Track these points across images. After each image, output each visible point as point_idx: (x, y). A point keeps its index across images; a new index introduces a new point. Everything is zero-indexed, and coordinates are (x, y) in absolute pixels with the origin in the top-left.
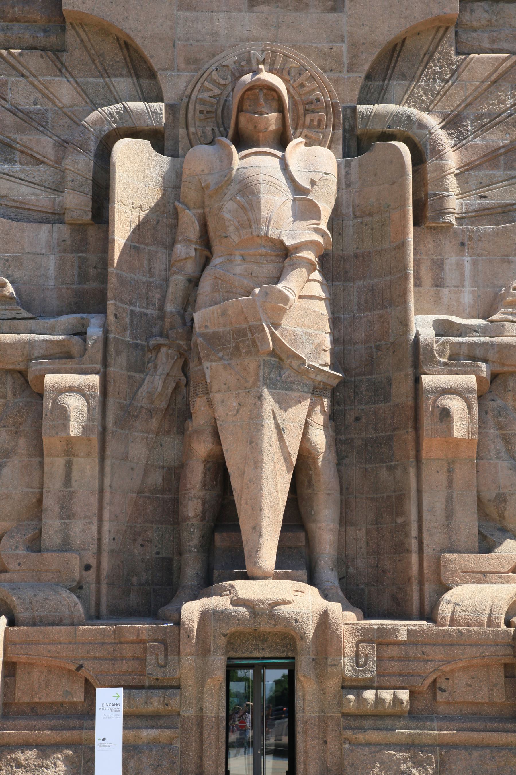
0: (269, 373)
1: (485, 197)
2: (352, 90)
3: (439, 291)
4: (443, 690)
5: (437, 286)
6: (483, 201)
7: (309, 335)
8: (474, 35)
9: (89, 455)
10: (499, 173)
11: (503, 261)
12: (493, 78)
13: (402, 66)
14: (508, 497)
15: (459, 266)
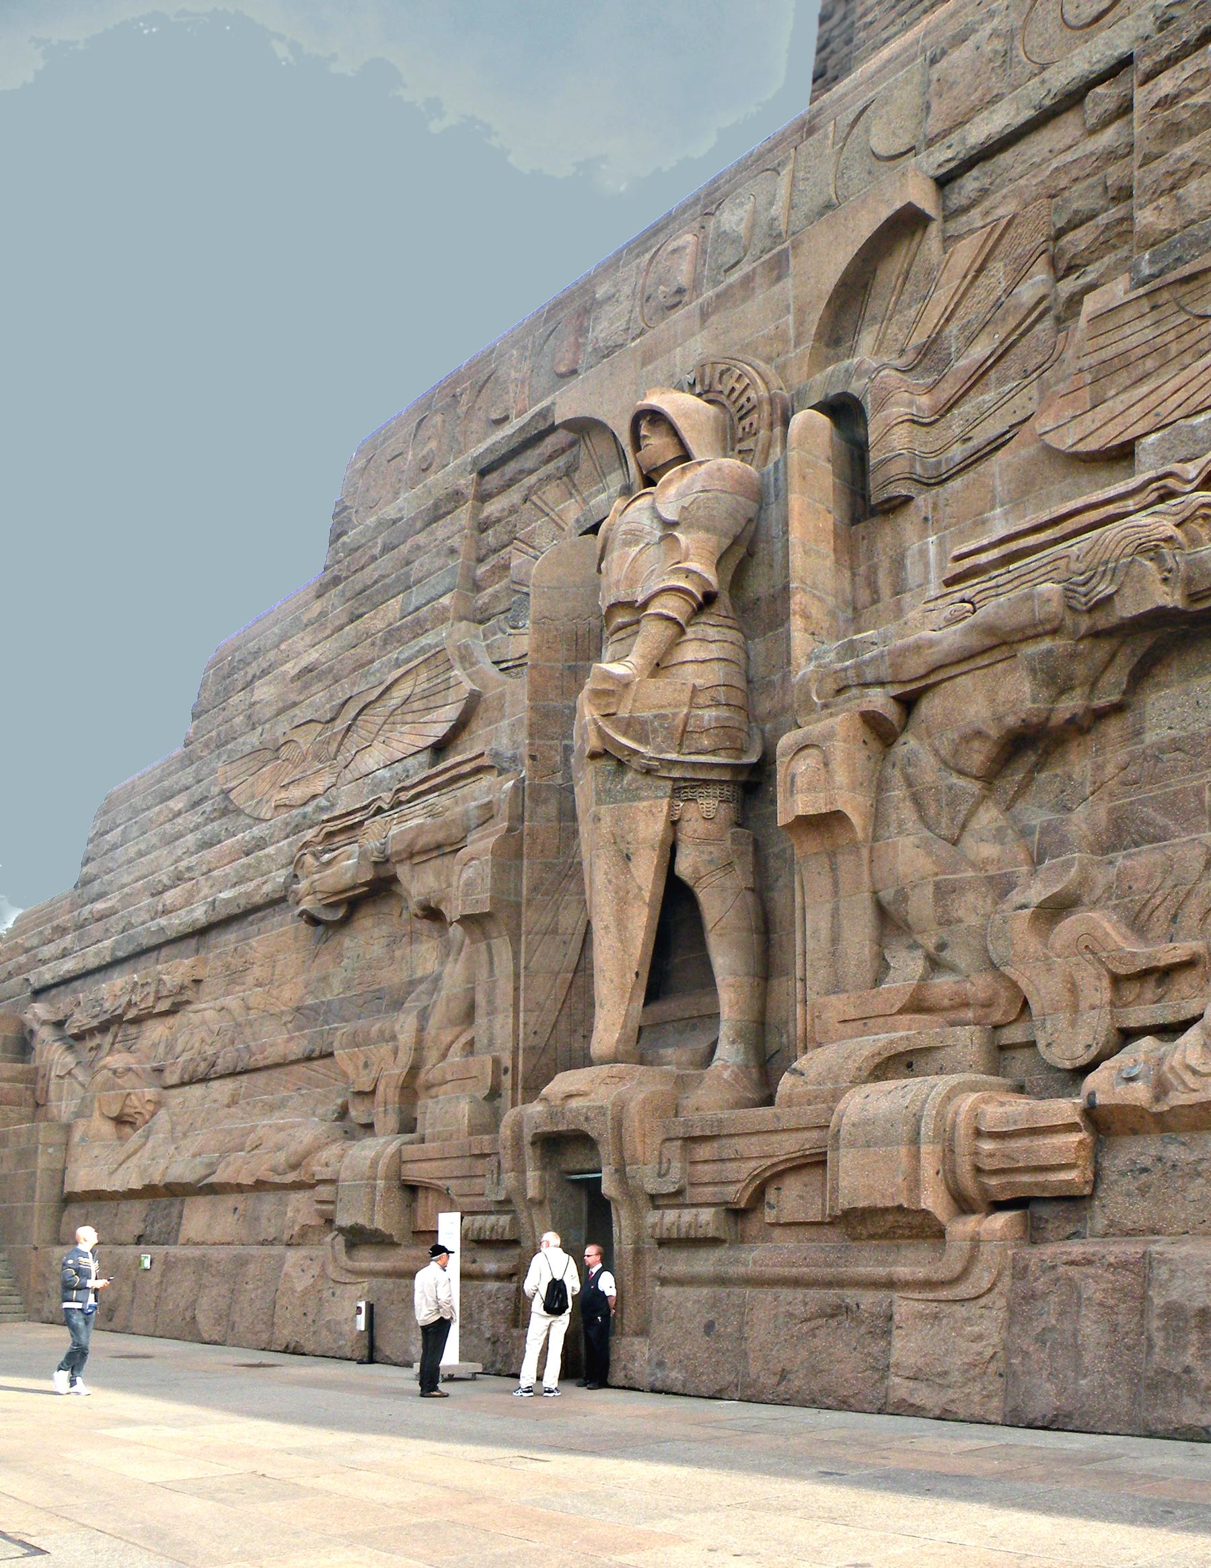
0: (603, 785)
1: (970, 438)
2: (799, 369)
3: (899, 601)
4: (771, 1207)
5: (898, 594)
6: (970, 444)
7: (664, 717)
8: (964, 218)
9: (500, 935)
10: (990, 396)
11: (976, 524)
12: (976, 265)
13: (875, 307)
14: (910, 893)
15: (923, 553)
